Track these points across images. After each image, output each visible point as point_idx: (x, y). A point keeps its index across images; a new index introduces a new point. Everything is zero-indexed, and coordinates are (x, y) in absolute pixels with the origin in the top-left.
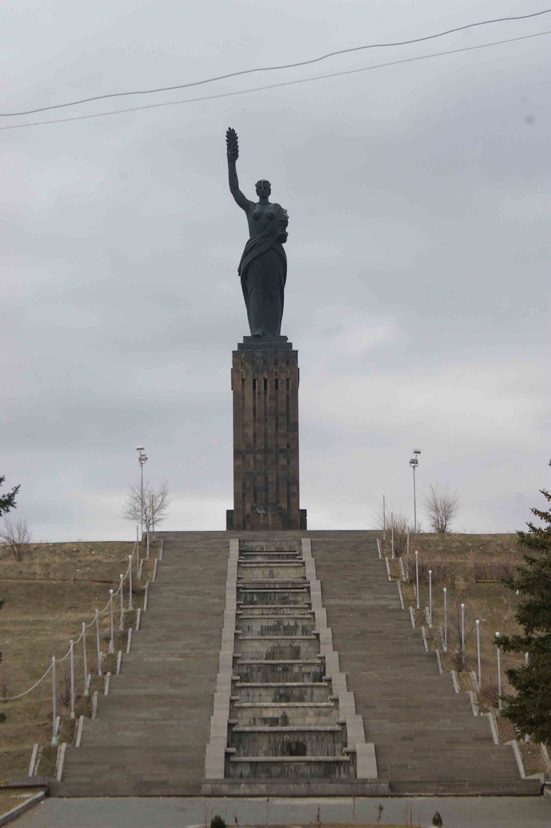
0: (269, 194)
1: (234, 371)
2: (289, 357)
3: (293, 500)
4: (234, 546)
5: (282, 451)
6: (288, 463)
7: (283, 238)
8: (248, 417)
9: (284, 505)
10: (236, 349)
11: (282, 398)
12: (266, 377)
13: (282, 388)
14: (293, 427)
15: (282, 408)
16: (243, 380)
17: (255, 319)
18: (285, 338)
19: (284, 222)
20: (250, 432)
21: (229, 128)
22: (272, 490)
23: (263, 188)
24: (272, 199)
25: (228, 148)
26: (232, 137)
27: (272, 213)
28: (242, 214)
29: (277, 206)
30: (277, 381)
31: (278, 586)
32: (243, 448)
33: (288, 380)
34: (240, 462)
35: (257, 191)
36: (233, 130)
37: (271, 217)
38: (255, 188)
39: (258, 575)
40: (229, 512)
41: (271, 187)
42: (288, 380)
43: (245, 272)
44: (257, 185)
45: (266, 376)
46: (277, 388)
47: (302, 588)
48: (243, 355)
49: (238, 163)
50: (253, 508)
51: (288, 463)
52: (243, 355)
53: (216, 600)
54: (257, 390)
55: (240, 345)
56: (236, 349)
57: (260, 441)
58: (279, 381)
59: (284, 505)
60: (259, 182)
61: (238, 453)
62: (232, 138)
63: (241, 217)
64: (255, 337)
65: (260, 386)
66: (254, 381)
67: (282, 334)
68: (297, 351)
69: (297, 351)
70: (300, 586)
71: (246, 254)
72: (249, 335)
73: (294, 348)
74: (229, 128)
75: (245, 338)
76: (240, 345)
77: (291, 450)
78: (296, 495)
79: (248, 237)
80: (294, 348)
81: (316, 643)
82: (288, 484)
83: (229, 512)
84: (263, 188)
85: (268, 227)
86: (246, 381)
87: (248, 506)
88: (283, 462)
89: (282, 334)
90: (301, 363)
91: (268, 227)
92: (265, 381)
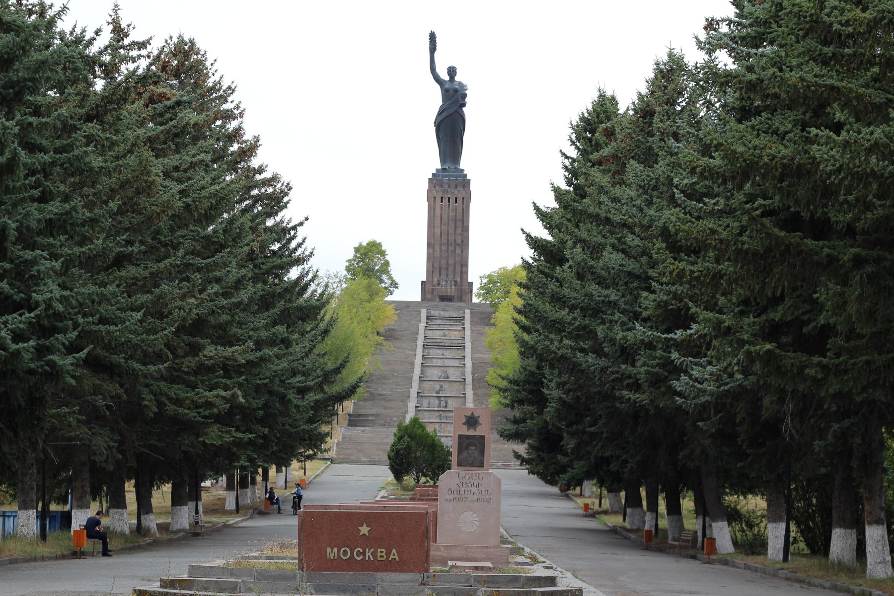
1: (429, 191)
2: (465, 183)
3: (464, 276)
4: (424, 313)
5: (458, 245)
6: (462, 252)
7: (464, 105)
8: (437, 222)
9: (458, 280)
11: (460, 210)
13: (460, 201)
14: (466, 229)
15: (459, 216)
17: (443, 159)
18: (463, 170)
19: (465, 96)
20: (438, 231)
22: (451, 269)
23: (452, 72)
24: (457, 78)
26: (433, 37)
28: (438, 87)
32: (433, 241)
34: (431, 251)
37: (456, 91)
39: (436, 335)
40: (423, 282)
43: (440, 125)
45: (450, 194)
49: (436, 54)
50: (439, 281)
51: (462, 252)
53: (411, 352)
57: (444, 237)
59: (458, 280)
61: (430, 245)
62: (433, 37)
64: (444, 170)
65: (445, 200)
67: (461, 167)
71: (439, 114)
72: (439, 167)
73: (468, 178)
75: (437, 170)
77: (463, 244)
78: (467, 273)
80: (468, 178)
81: (461, 387)
82: (462, 266)
83: (423, 282)
84: (452, 72)
87: (435, 279)
88: (458, 251)
89: (461, 167)
90: (473, 187)
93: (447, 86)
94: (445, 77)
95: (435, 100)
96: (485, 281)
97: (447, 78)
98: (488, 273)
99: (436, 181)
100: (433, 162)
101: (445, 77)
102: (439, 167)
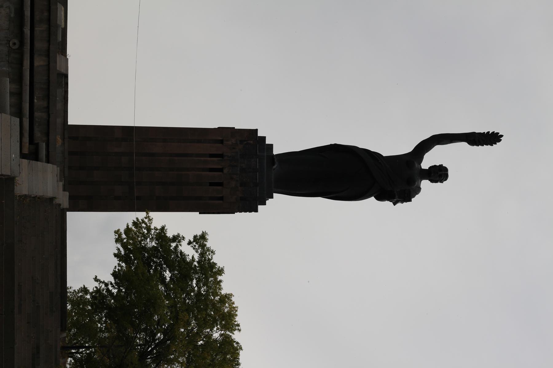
0: (432, 181)
10: (260, 134)
12: (225, 171)
16: (222, 142)
18: (272, 197)
21: (502, 136)
23: (439, 174)
24: (425, 184)
25: (480, 134)
26: (491, 139)
27: (414, 183)
29: (418, 190)
30: (220, 184)
31: (39, 62)
33: (221, 198)
35: (435, 166)
36: (500, 141)
38: (438, 165)
41: (439, 184)
42: (221, 198)
44: (441, 166)
46: (211, 184)
47: (31, 141)
48: (252, 142)
49: (464, 144)
52: (252, 142)
54: (209, 159)
55: (264, 138)
56: (260, 134)
58: (219, 188)
60: (446, 169)
62: (491, 139)
63: (405, 147)
66: (221, 156)
68: (256, 211)
69: (256, 211)
70: (38, 134)
72: (276, 152)
73: (260, 207)
74: (502, 136)
76: (264, 138)
79: (384, 155)
80: (260, 207)
84: (439, 174)
85: (391, 178)
86: (220, 145)
89: (275, 195)
91: (391, 178)
92: (221, 170)
93: (416, 165)
94: (428, 161)
95: (391, 143)
96: (190, 252)
97: (426, 164)
98: (217, 260)
99: (249, 142)
100: (286, 138)
101: (428, 161)
102: (276, 152)
